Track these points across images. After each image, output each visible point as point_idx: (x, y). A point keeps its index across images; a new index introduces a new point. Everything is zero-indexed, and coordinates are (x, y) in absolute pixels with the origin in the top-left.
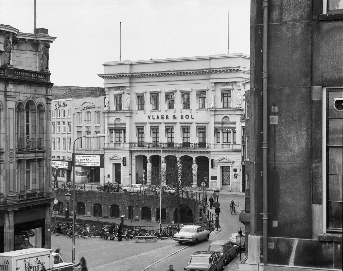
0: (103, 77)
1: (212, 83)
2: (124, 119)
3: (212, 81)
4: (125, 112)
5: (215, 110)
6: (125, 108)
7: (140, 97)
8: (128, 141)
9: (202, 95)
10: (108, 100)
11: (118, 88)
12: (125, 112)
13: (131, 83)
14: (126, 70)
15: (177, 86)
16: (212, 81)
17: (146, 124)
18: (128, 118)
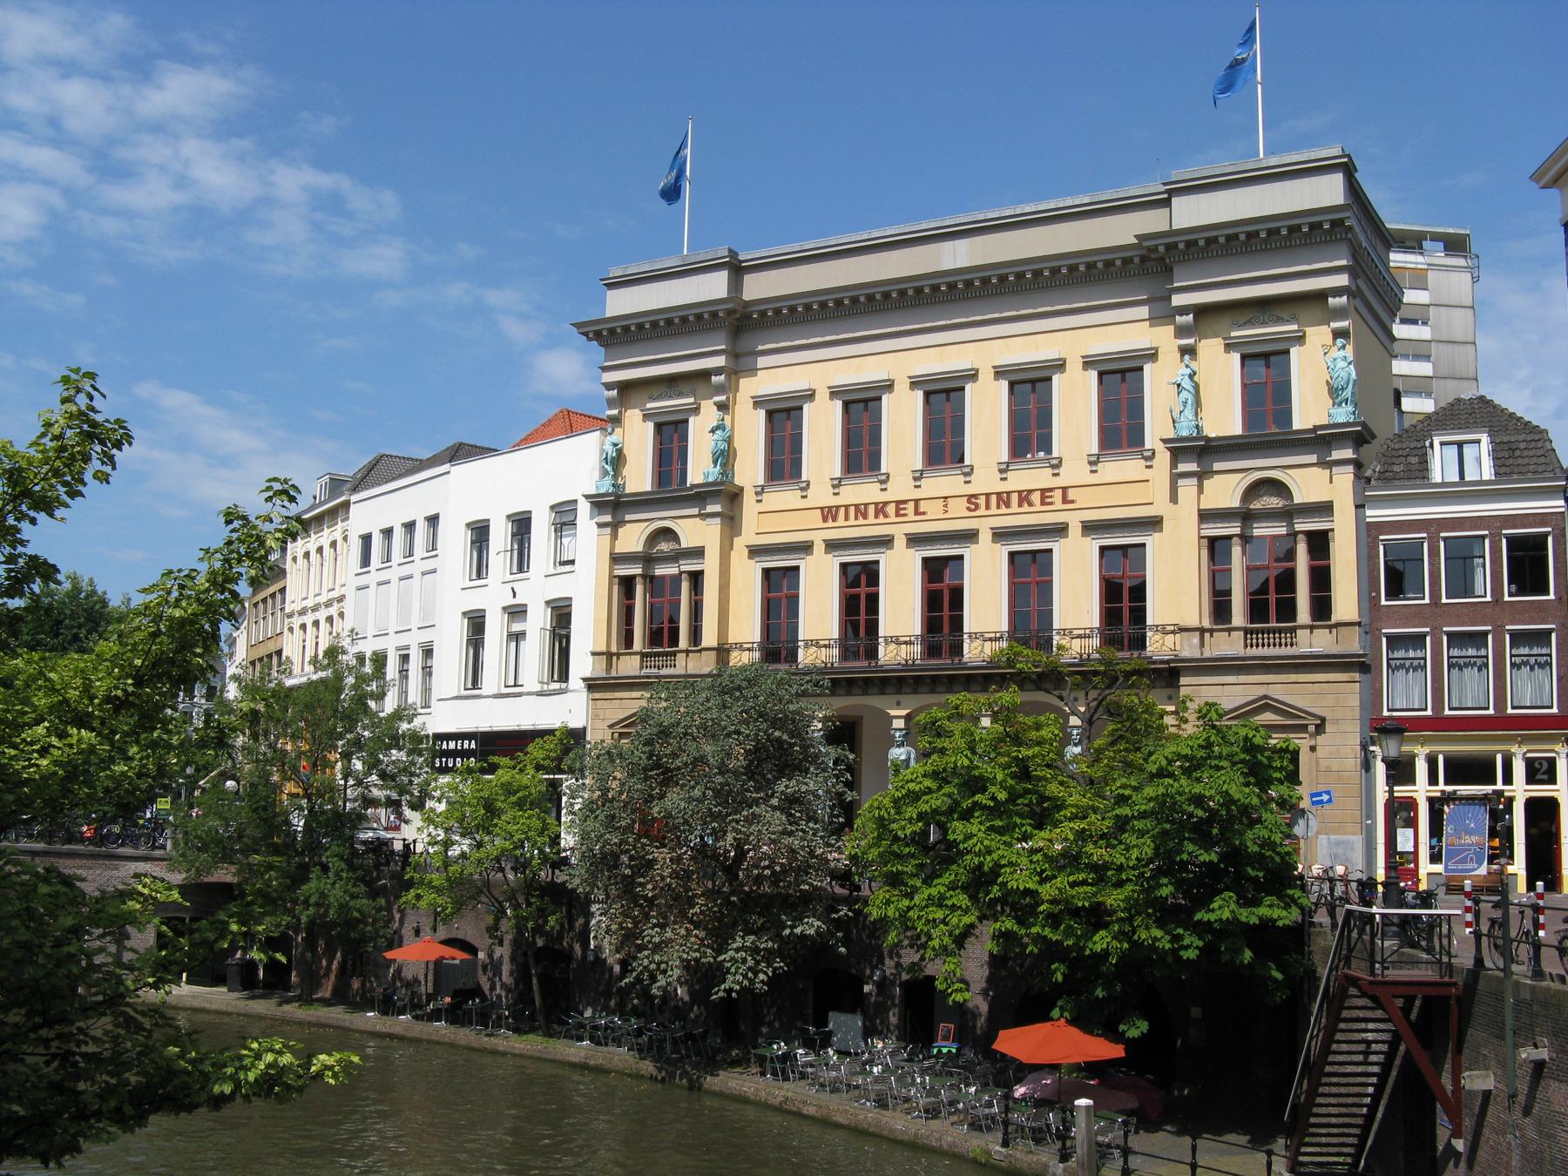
0: (598, 336)
1: (1183, 310)
2: (696, 530)
3: (1178, 300)
4: (700, 496)
5: (1199, 453)
6: (700, 468)
7: (783, 417)
8: (709, 638)
9: (1120, 378)
10: (615, 445)
11: (671, 383)
12: (700, 496)
13: (734, 355)
14: (714, 287)
15: (984, 350)
16: (1178, 300)
17: (806, 548)
18: (718, 520)
